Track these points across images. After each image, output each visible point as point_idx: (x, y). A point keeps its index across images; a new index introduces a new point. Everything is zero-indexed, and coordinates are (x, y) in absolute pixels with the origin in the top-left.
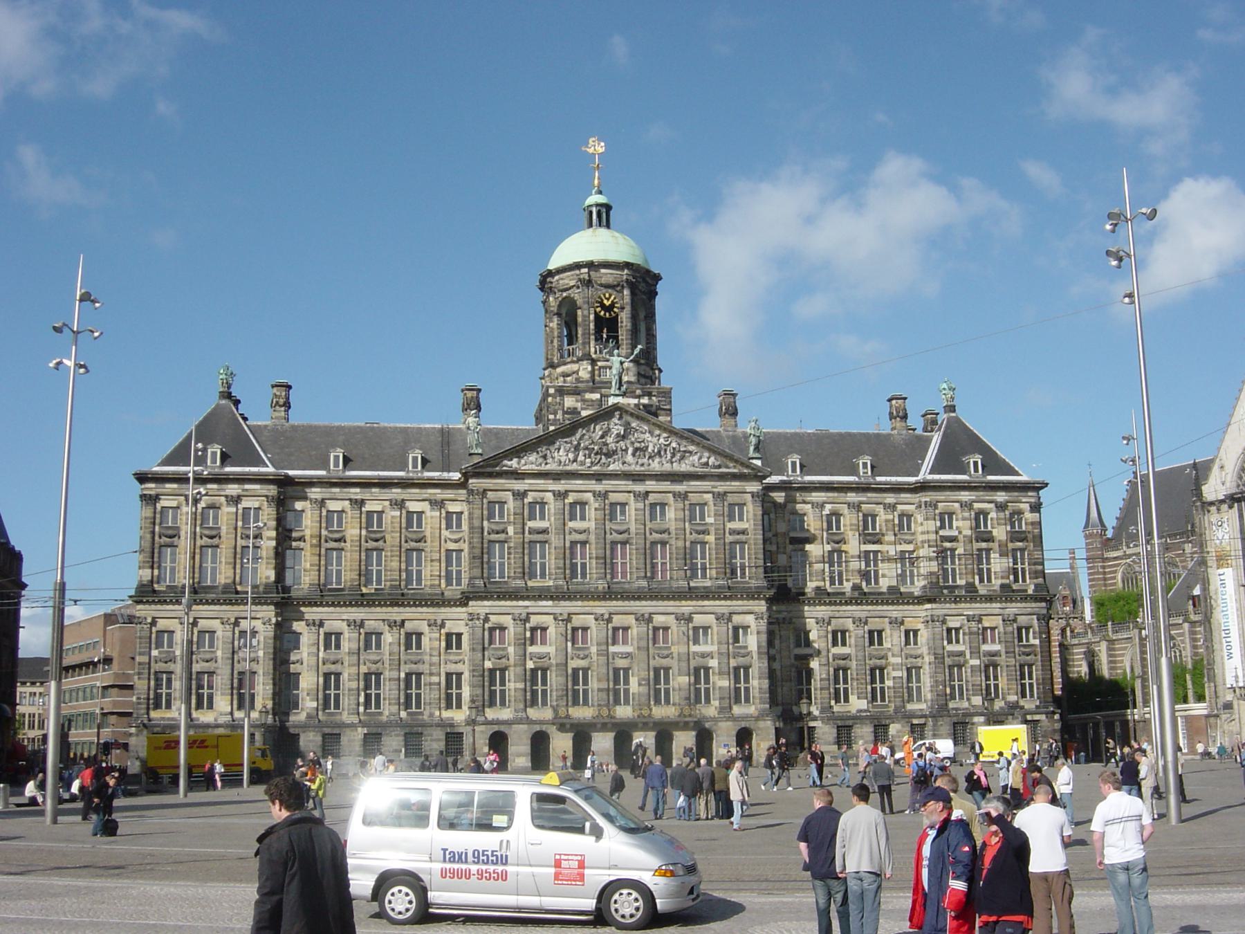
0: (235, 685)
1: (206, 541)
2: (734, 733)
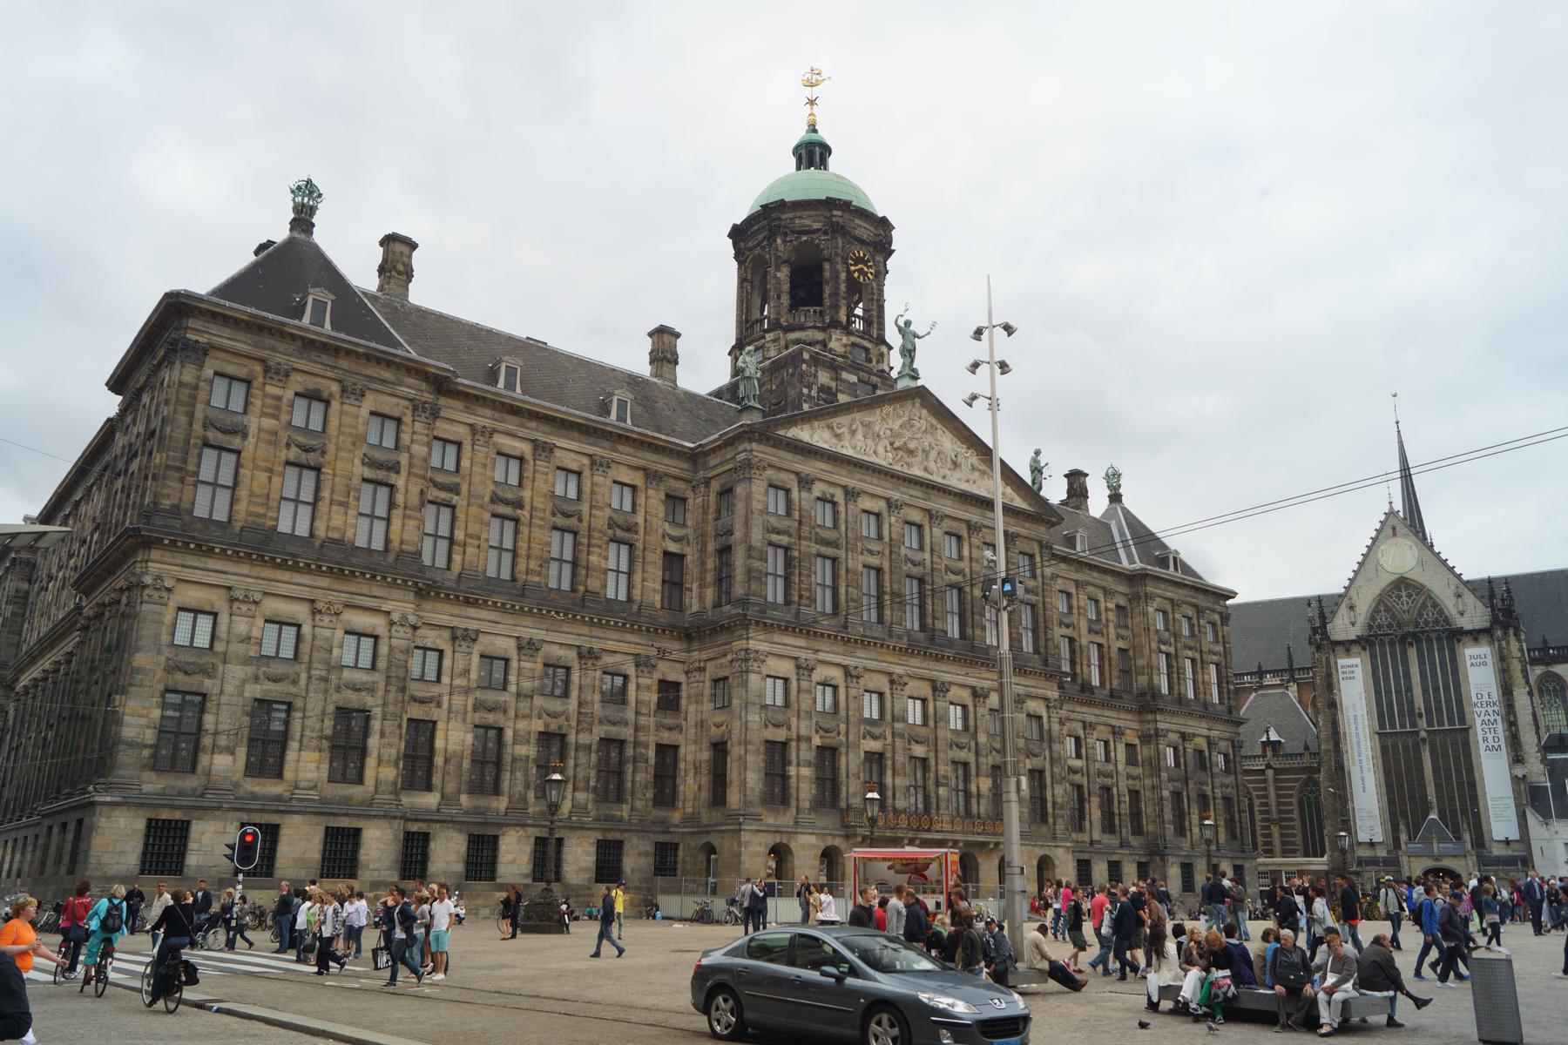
0: (328, 732)
1: (293, 454)
2: (1035, 862)
